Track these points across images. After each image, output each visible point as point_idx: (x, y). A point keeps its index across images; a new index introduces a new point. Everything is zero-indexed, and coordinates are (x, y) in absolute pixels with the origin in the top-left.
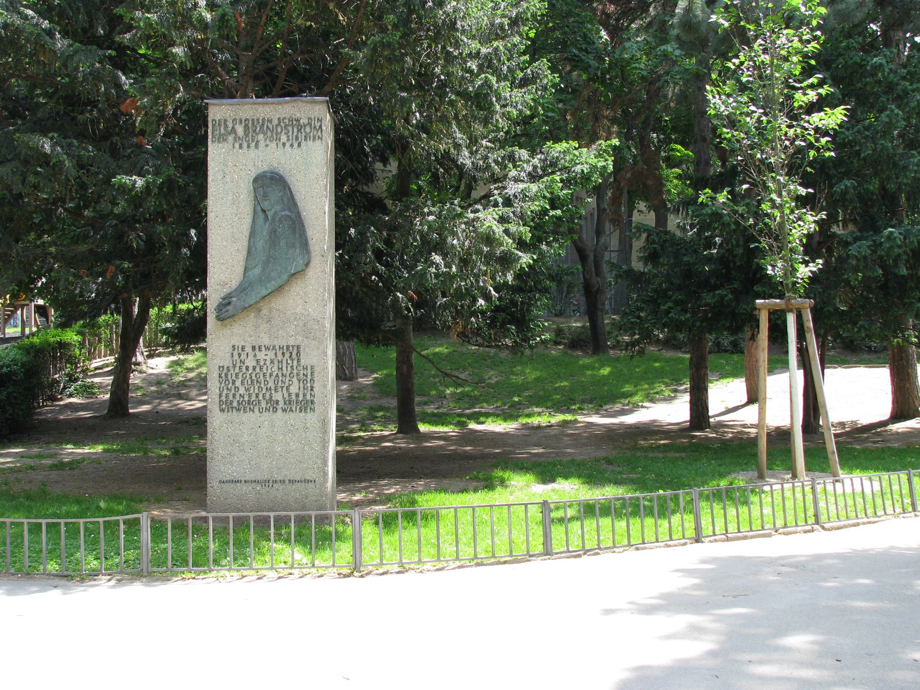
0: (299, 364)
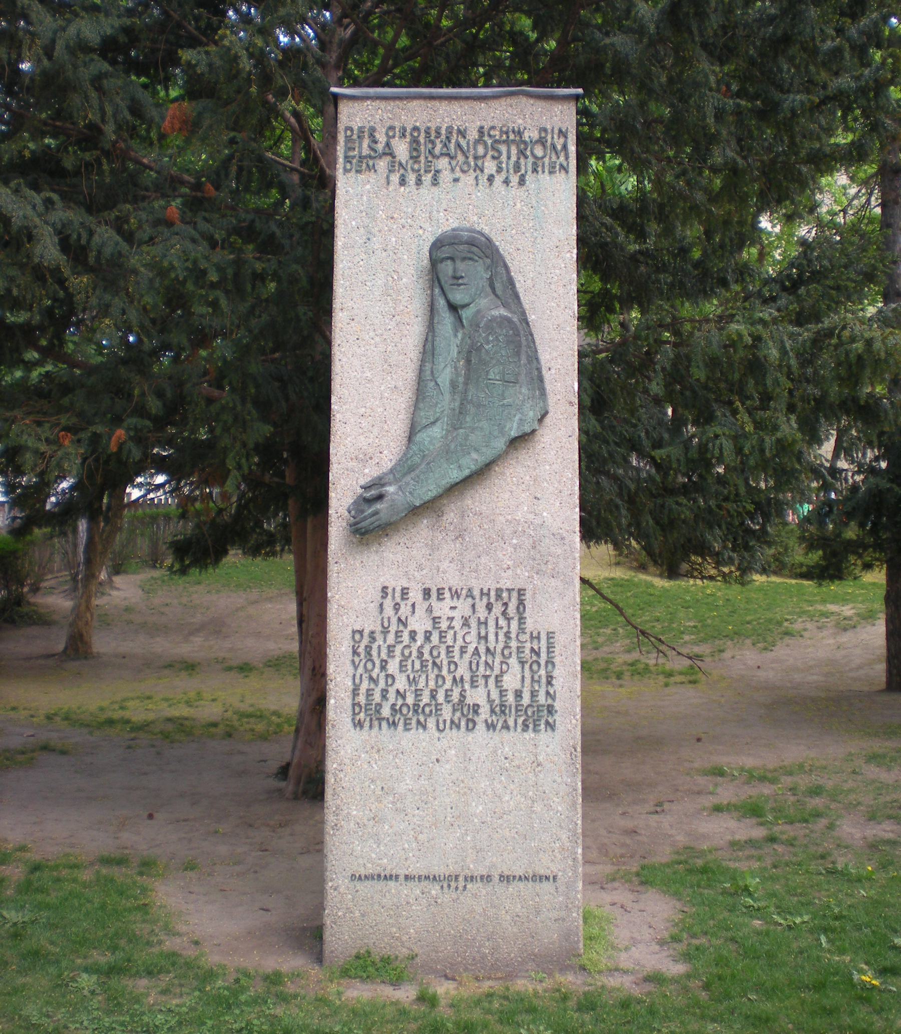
0: (521, 630)
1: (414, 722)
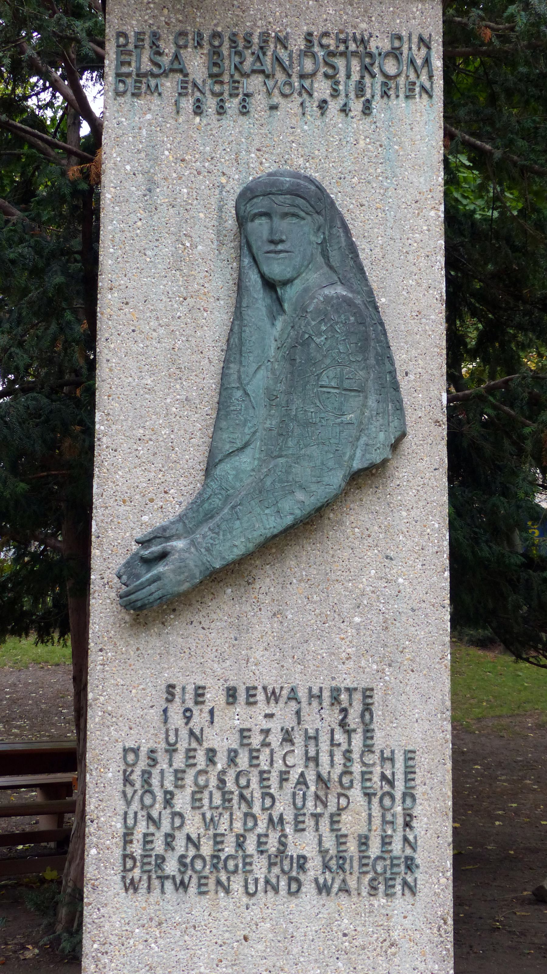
0: (368, 748)
1: (212, 882)
